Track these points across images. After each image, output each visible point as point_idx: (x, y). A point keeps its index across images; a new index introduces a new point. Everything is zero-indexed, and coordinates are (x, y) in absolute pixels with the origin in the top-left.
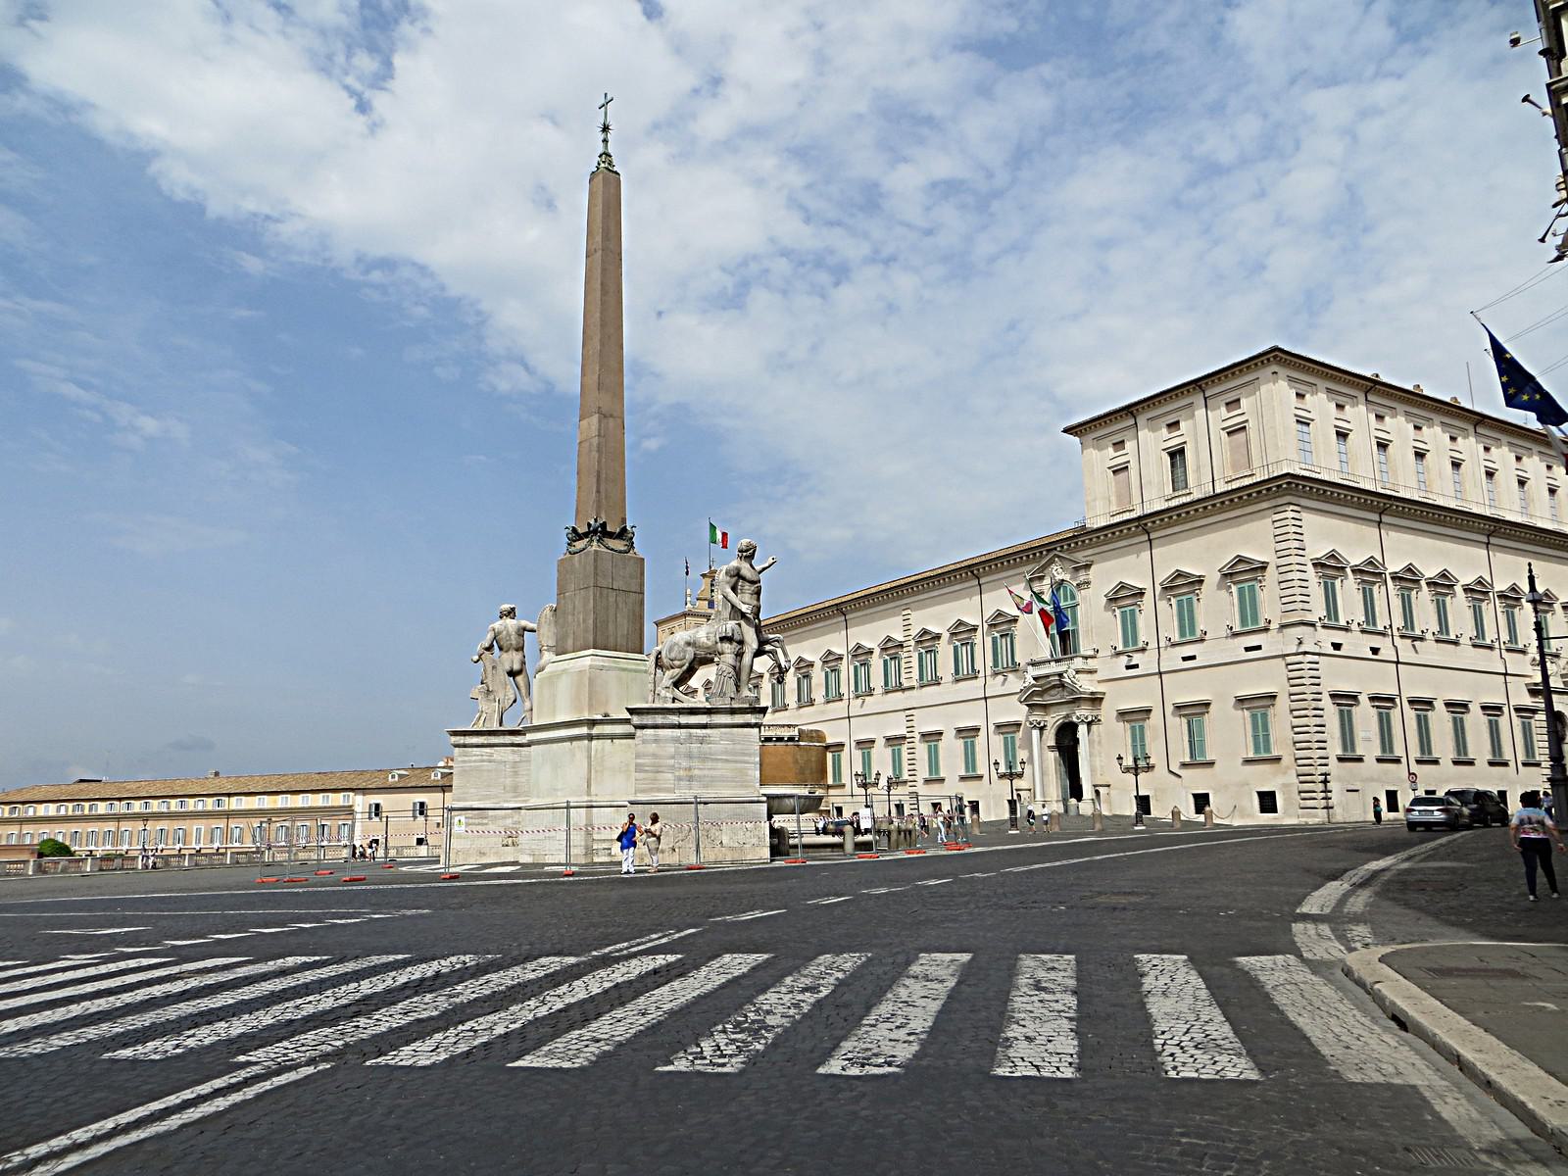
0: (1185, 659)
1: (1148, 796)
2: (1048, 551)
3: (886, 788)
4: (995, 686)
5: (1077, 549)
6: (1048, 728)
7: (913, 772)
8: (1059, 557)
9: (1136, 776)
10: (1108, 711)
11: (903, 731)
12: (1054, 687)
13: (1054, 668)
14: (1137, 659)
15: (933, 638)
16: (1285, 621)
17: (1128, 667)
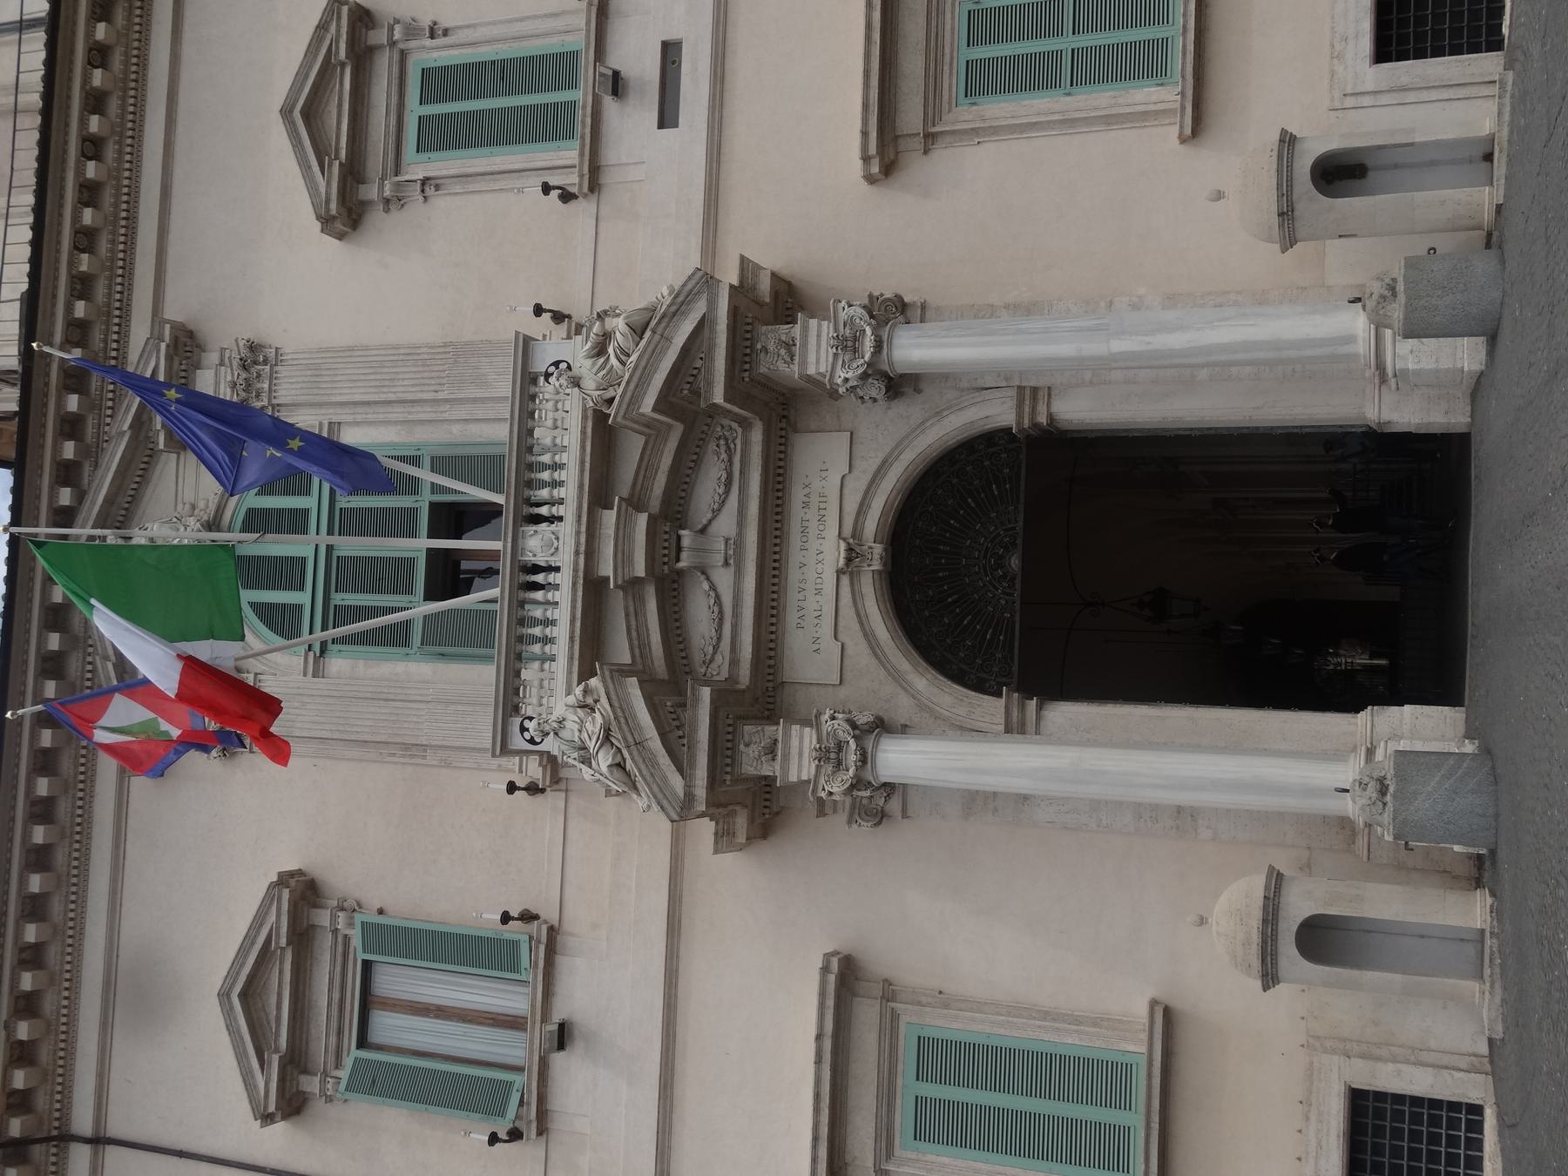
17: (667, 118)
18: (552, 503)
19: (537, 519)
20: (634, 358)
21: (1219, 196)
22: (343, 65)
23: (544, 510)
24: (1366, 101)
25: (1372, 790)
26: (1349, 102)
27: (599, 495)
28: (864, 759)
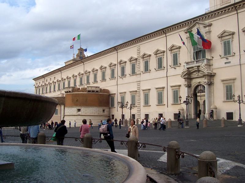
1: (232, 113)
2: (194, 21)
3: (130, 108)
4: (171, 71)
5: (205, 20)
6: (192, 87)
8: (198, 23)
9: (240, 104)
10: (217, 81)
11: (136, 89)
12: (195, 71)
13: (195, 64)
15: (148, 56)
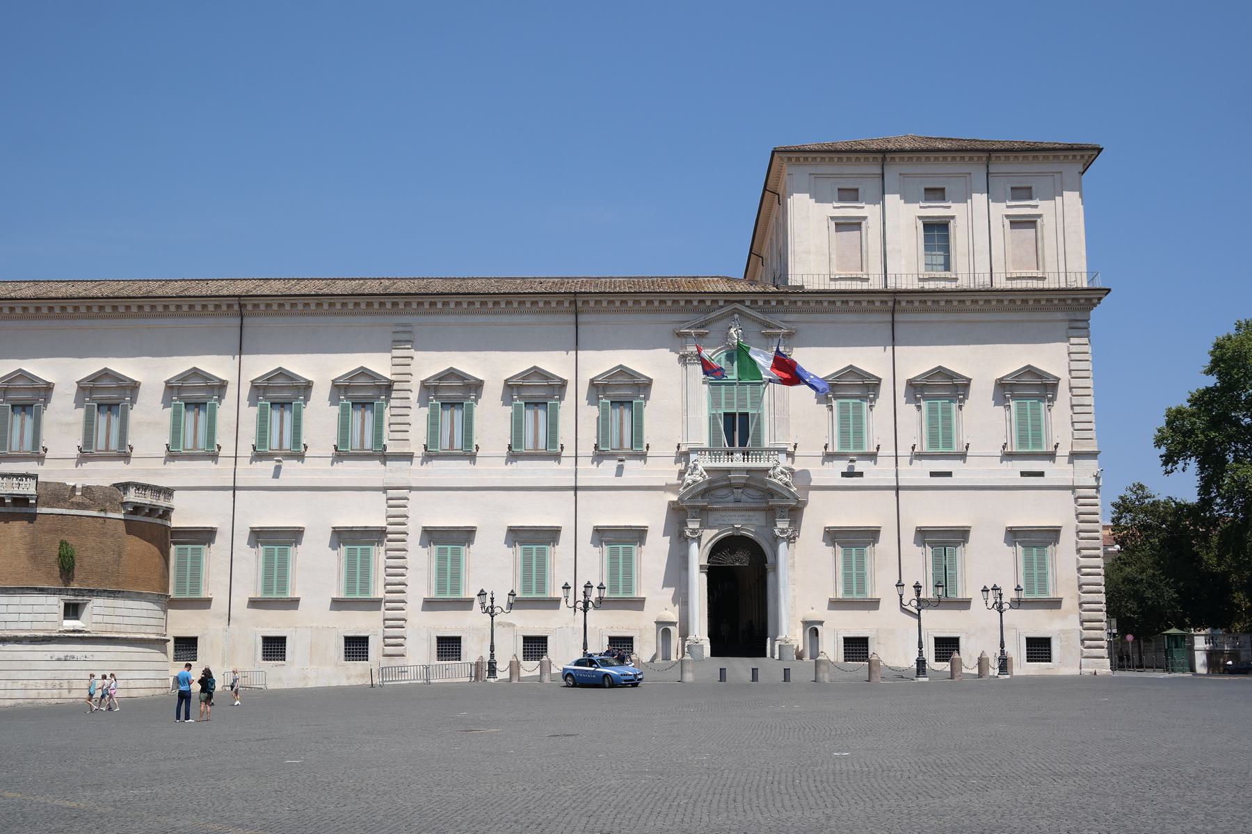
0: (933, 474)
7: (397, 587)
8: (741, 313)
11: (381, 522)
13: (738, 462)
14: (859, 466)
16: (1076, 449)
17: (844, 475)
18: (748, 459)
19: (744, 454)
20: (780, 483)
21: (812, 608)
22: (863, 381)
23: (746, 457)
24: (836, 636)
25: (696, 641)
26: (836, 633)
27: (749, 471)
28: (694, 538)
